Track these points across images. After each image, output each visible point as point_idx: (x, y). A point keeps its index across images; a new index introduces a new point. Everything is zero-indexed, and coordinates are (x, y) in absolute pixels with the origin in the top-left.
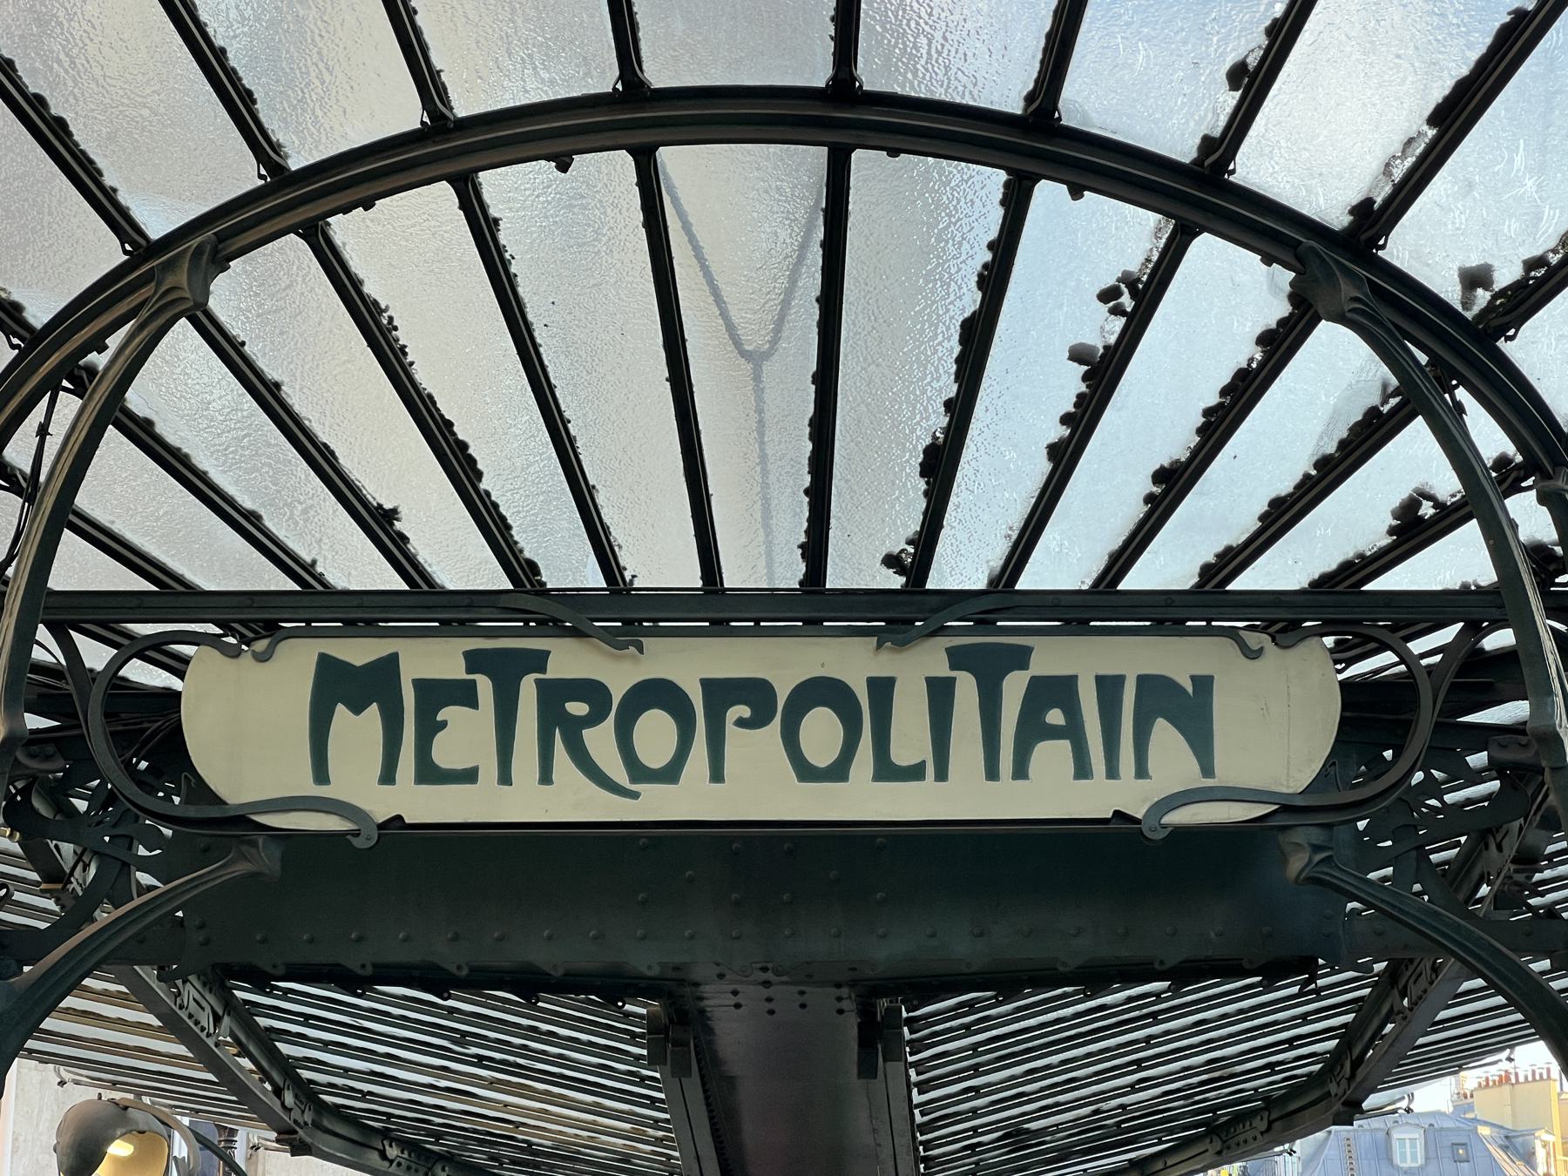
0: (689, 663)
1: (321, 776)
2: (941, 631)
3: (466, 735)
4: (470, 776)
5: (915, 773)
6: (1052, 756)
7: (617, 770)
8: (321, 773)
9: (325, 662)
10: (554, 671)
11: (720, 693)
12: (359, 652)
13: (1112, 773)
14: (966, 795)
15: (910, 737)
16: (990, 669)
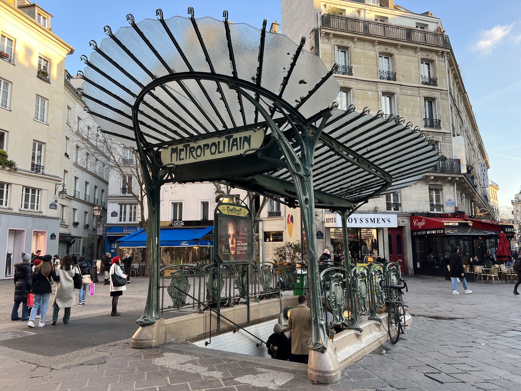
0: (202, 143)
3: (183, 154)
4: (183, 159)
5: (221, 152)
7: (195, 156)
11: (205, 146)
12: (174, 147)
14: (227, 154)
15: (221, 149)
16: (228, 138)
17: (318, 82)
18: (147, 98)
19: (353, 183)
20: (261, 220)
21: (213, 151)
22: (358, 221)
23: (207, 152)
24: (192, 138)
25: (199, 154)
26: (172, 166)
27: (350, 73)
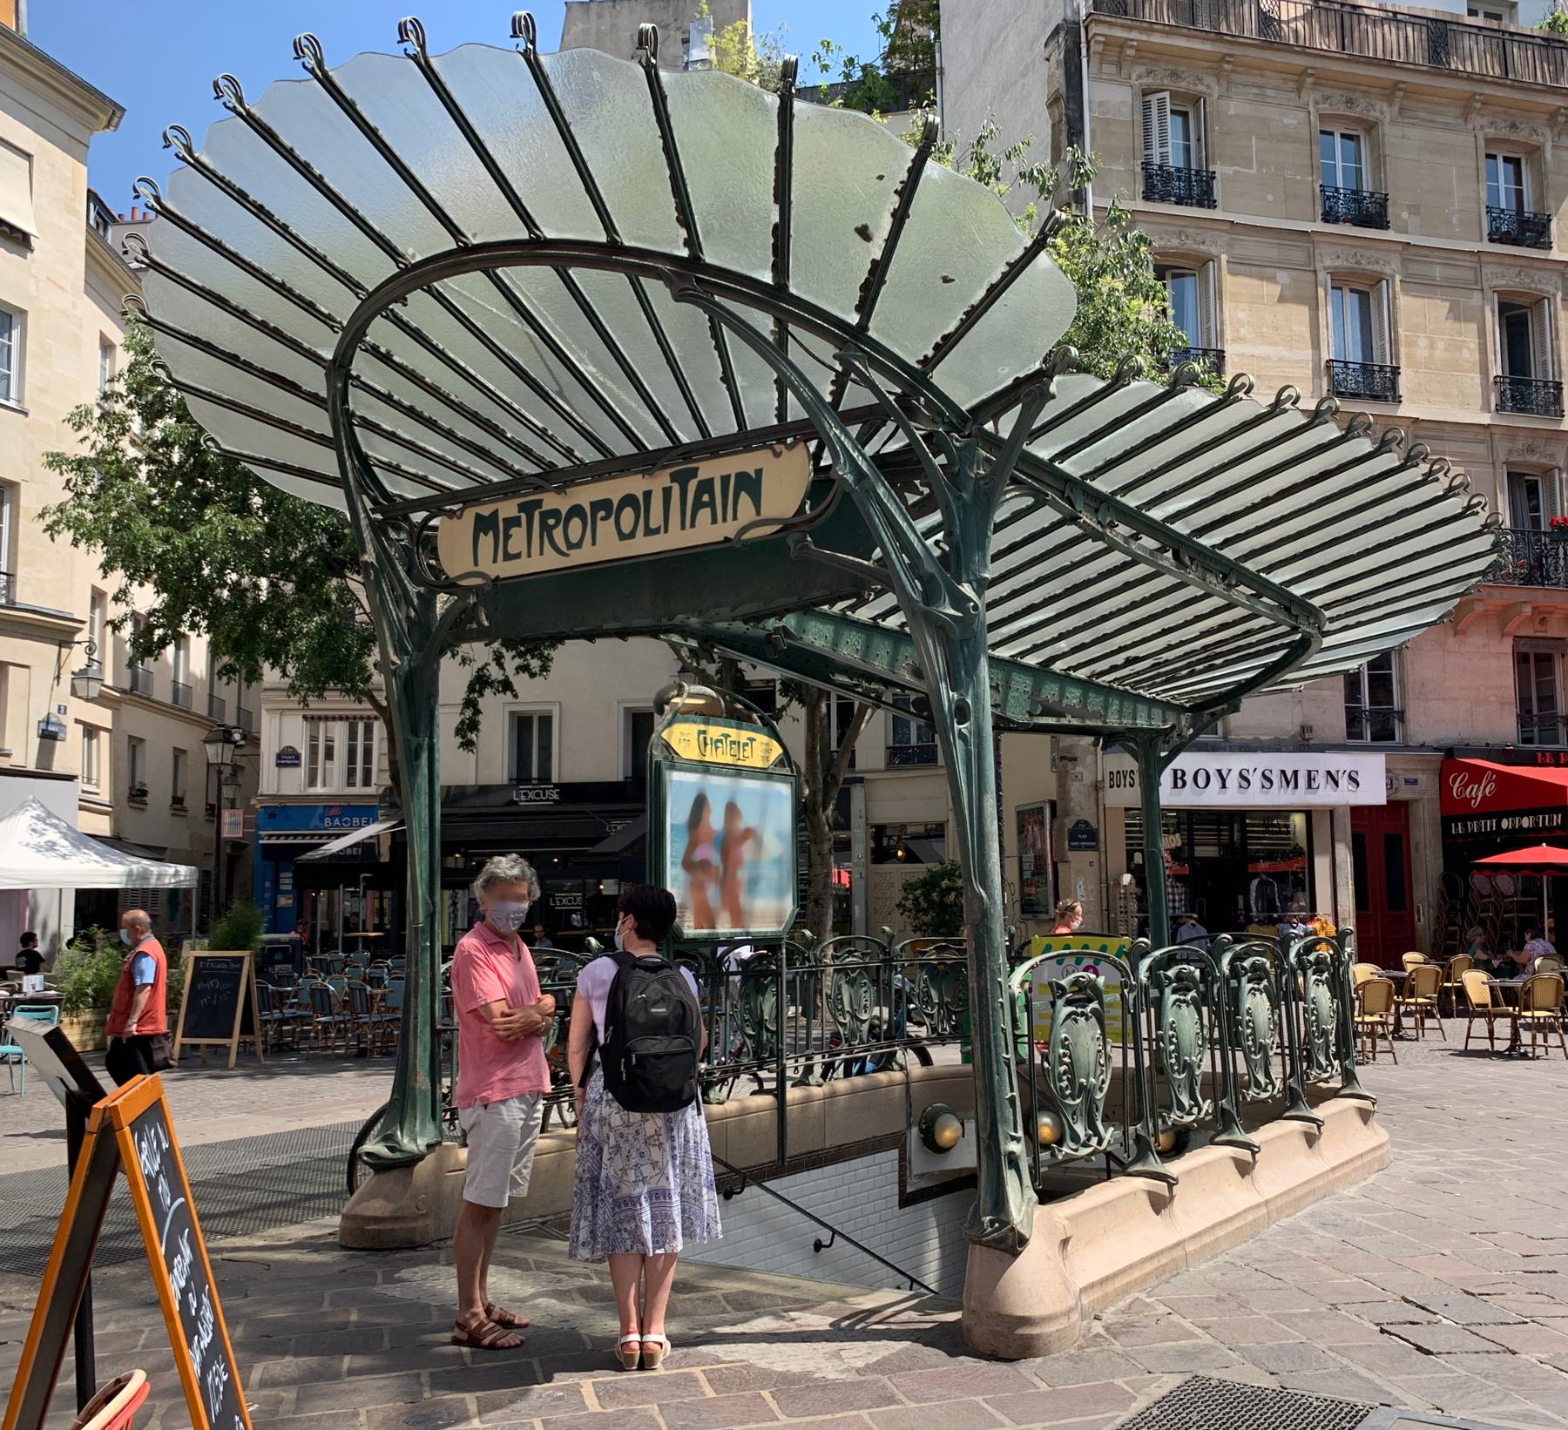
0: (585, 495)
1: (476, 564)
2: (666, 467)
4: (518, 556)
5: (657, 531)
6: (705, 513)
7: (563, 548)
8: (476, 564)
9: (478, 516)
10: (545, 507)
11: (596, 506)
12: (486, 510)
13: (725, 520)
17: (995, 277)
18: (380, 332)
19: (1172, 638)
20: (861, 780)
21: (626, 529)
22: (1233, 780)
23: (606, 528)
24: (551, 477)
25: (574, 539)
26: (478, 581)
27: (1206, 199)
